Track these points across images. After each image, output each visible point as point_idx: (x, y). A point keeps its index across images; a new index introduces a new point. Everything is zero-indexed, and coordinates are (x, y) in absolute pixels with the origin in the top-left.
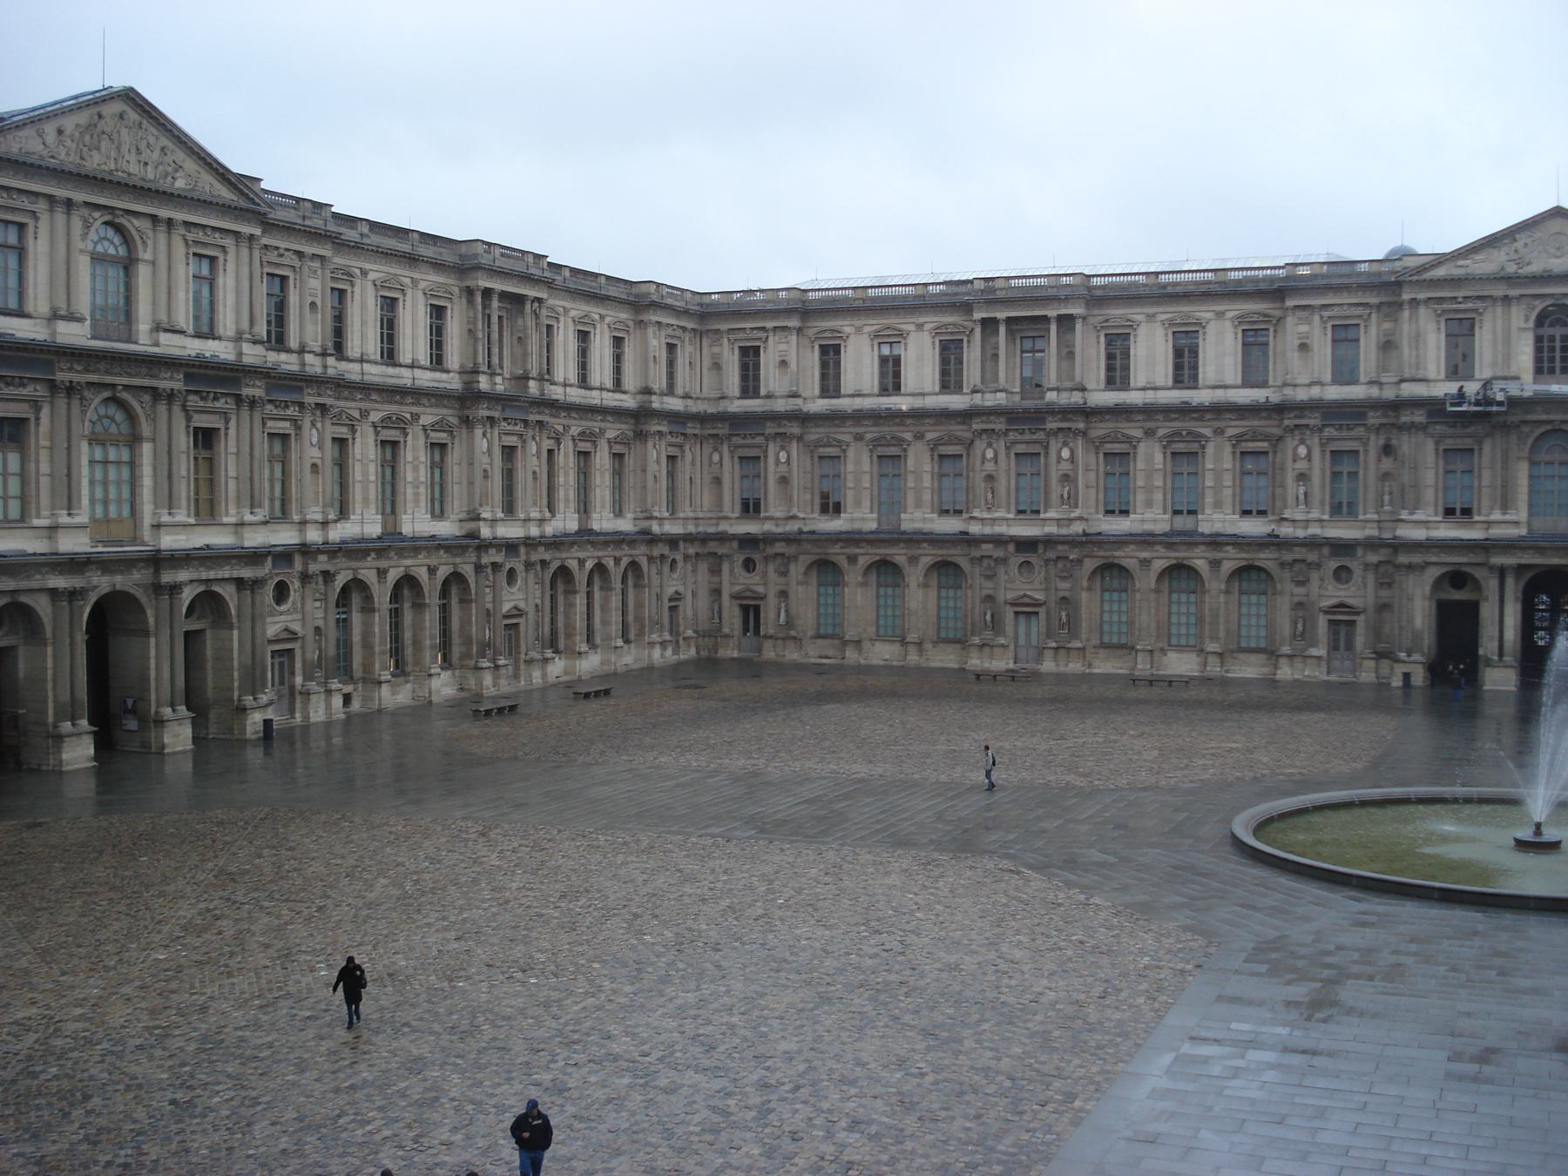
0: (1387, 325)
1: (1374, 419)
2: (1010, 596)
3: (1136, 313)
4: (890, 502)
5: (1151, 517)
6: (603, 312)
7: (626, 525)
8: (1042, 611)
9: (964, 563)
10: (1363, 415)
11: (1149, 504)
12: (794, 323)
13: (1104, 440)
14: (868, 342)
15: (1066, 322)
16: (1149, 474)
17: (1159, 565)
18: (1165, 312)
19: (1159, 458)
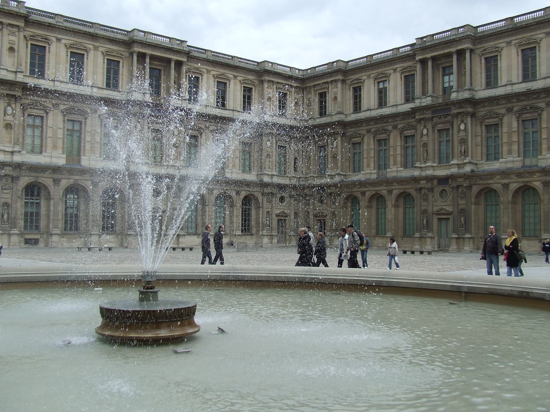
2: (435, 209)
3: (501, 43)
4: (382, 165)
5: (511, 160)
6: (236, 74)
7: (251, 177)
8: (451, 217)
9: (413, 193)
11: (510, 152)
12: (340, 77)
13: (484, 118)
14: (373, 82)
15: (461, 53)
16: (510, 135)
17: (514, 186)
18: (515, 39)
19: (515, 124)
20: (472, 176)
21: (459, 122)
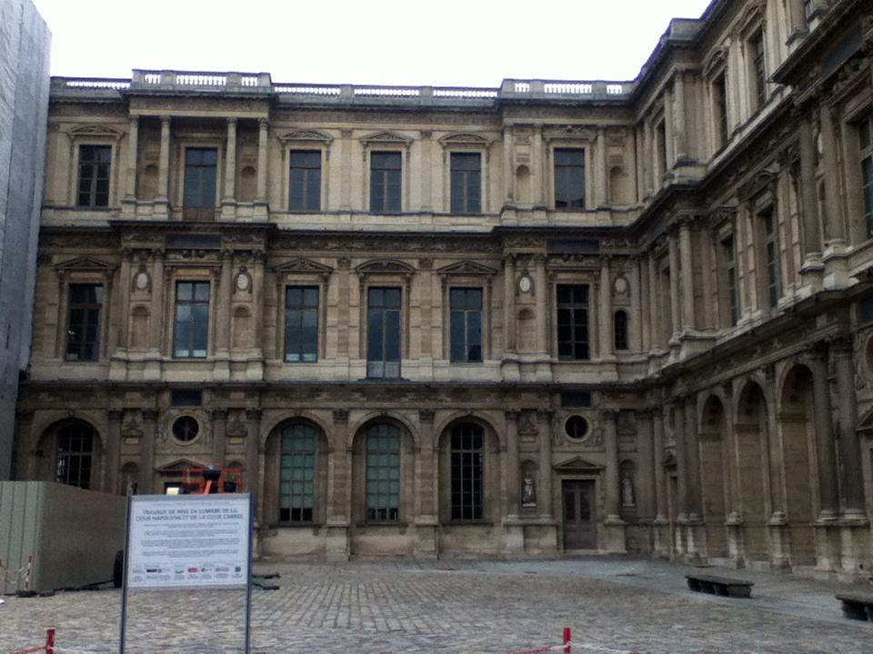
0: (615, 151)
1: (606, 248)
3: (331, 127)
5: (340, 362)
10: (596, 244)
15: (248, 129)
17: (358, 418)
20: (260, 390)
21: (236, 271)
